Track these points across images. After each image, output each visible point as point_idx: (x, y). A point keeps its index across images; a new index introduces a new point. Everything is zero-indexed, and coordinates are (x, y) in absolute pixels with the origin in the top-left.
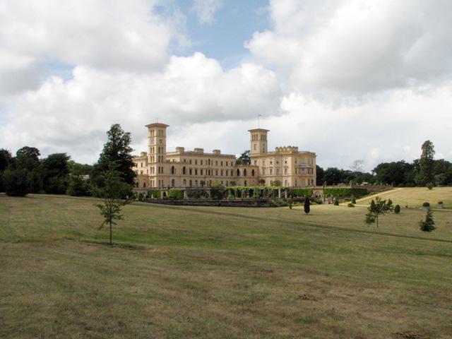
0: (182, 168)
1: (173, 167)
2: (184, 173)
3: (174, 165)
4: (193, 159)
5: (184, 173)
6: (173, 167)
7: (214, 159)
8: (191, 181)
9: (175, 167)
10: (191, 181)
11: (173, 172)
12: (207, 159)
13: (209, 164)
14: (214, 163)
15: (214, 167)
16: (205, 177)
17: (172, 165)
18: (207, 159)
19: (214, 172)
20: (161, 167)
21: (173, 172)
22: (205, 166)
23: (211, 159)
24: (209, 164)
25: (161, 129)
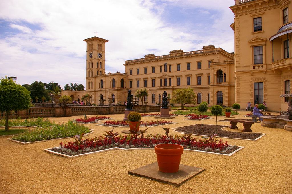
0: (111, 80)
1: (102, 81)
2: (113, 86)
3: (103, 79)
4: (142, 67)
5: (113, 86)
6: (102, 81)
7: (174, 63)
8: (153, 95)
9: (104, 81)
10: (153, 95)
11: (102, 87)
12: (162, 63)
13: (165, 71)
14: (174, 68)
15: (174, 73)
16: (156, 90)
17: (100, 79)
18: (162, 63)
19: (174, 82)
20: (90, 81)
21: (102, 87)
22: (158, 74)
23: (168, 63)
24: (165, 71)
25: (100, 43)
